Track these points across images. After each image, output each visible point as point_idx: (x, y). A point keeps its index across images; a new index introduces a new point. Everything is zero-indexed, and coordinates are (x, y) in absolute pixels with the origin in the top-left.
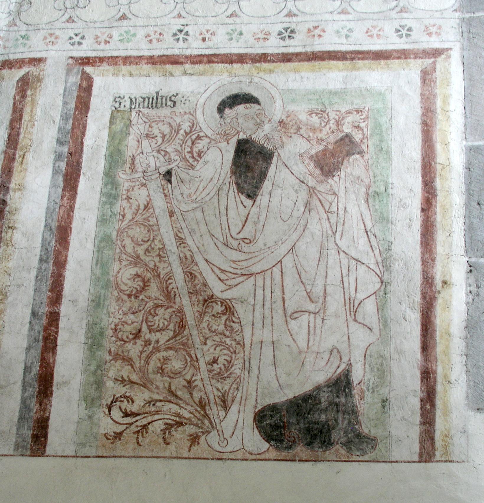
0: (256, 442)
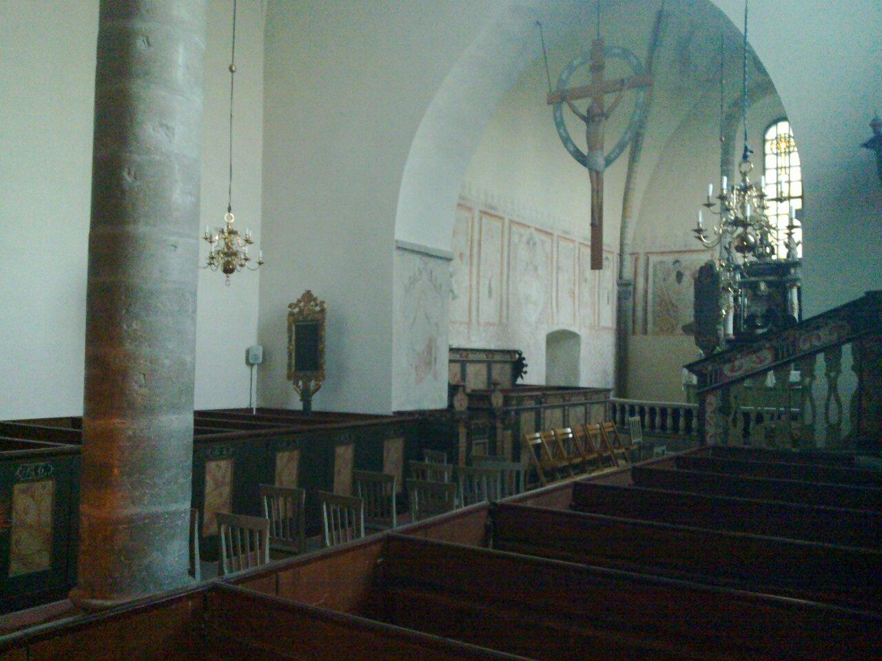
0: (681, 332)
